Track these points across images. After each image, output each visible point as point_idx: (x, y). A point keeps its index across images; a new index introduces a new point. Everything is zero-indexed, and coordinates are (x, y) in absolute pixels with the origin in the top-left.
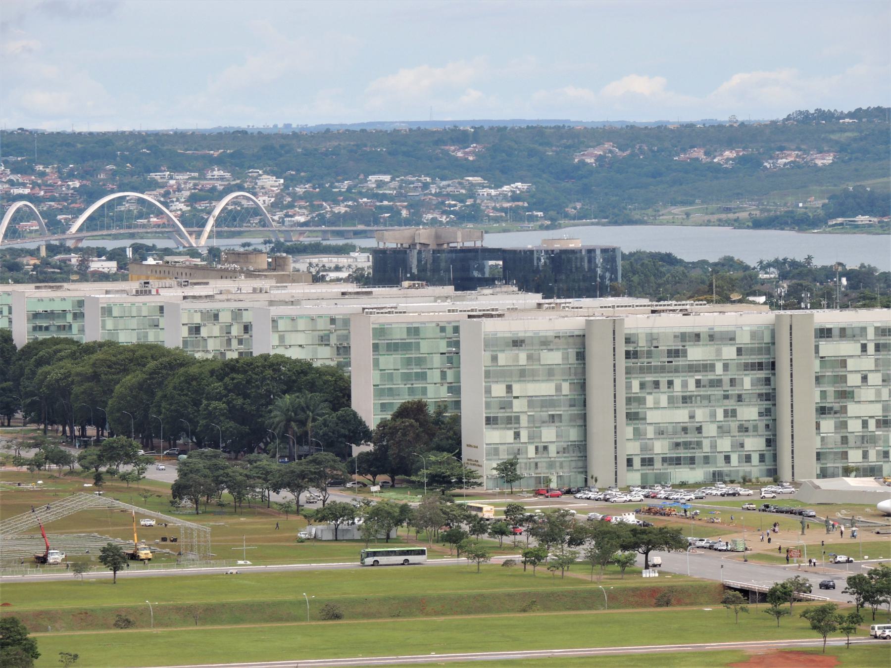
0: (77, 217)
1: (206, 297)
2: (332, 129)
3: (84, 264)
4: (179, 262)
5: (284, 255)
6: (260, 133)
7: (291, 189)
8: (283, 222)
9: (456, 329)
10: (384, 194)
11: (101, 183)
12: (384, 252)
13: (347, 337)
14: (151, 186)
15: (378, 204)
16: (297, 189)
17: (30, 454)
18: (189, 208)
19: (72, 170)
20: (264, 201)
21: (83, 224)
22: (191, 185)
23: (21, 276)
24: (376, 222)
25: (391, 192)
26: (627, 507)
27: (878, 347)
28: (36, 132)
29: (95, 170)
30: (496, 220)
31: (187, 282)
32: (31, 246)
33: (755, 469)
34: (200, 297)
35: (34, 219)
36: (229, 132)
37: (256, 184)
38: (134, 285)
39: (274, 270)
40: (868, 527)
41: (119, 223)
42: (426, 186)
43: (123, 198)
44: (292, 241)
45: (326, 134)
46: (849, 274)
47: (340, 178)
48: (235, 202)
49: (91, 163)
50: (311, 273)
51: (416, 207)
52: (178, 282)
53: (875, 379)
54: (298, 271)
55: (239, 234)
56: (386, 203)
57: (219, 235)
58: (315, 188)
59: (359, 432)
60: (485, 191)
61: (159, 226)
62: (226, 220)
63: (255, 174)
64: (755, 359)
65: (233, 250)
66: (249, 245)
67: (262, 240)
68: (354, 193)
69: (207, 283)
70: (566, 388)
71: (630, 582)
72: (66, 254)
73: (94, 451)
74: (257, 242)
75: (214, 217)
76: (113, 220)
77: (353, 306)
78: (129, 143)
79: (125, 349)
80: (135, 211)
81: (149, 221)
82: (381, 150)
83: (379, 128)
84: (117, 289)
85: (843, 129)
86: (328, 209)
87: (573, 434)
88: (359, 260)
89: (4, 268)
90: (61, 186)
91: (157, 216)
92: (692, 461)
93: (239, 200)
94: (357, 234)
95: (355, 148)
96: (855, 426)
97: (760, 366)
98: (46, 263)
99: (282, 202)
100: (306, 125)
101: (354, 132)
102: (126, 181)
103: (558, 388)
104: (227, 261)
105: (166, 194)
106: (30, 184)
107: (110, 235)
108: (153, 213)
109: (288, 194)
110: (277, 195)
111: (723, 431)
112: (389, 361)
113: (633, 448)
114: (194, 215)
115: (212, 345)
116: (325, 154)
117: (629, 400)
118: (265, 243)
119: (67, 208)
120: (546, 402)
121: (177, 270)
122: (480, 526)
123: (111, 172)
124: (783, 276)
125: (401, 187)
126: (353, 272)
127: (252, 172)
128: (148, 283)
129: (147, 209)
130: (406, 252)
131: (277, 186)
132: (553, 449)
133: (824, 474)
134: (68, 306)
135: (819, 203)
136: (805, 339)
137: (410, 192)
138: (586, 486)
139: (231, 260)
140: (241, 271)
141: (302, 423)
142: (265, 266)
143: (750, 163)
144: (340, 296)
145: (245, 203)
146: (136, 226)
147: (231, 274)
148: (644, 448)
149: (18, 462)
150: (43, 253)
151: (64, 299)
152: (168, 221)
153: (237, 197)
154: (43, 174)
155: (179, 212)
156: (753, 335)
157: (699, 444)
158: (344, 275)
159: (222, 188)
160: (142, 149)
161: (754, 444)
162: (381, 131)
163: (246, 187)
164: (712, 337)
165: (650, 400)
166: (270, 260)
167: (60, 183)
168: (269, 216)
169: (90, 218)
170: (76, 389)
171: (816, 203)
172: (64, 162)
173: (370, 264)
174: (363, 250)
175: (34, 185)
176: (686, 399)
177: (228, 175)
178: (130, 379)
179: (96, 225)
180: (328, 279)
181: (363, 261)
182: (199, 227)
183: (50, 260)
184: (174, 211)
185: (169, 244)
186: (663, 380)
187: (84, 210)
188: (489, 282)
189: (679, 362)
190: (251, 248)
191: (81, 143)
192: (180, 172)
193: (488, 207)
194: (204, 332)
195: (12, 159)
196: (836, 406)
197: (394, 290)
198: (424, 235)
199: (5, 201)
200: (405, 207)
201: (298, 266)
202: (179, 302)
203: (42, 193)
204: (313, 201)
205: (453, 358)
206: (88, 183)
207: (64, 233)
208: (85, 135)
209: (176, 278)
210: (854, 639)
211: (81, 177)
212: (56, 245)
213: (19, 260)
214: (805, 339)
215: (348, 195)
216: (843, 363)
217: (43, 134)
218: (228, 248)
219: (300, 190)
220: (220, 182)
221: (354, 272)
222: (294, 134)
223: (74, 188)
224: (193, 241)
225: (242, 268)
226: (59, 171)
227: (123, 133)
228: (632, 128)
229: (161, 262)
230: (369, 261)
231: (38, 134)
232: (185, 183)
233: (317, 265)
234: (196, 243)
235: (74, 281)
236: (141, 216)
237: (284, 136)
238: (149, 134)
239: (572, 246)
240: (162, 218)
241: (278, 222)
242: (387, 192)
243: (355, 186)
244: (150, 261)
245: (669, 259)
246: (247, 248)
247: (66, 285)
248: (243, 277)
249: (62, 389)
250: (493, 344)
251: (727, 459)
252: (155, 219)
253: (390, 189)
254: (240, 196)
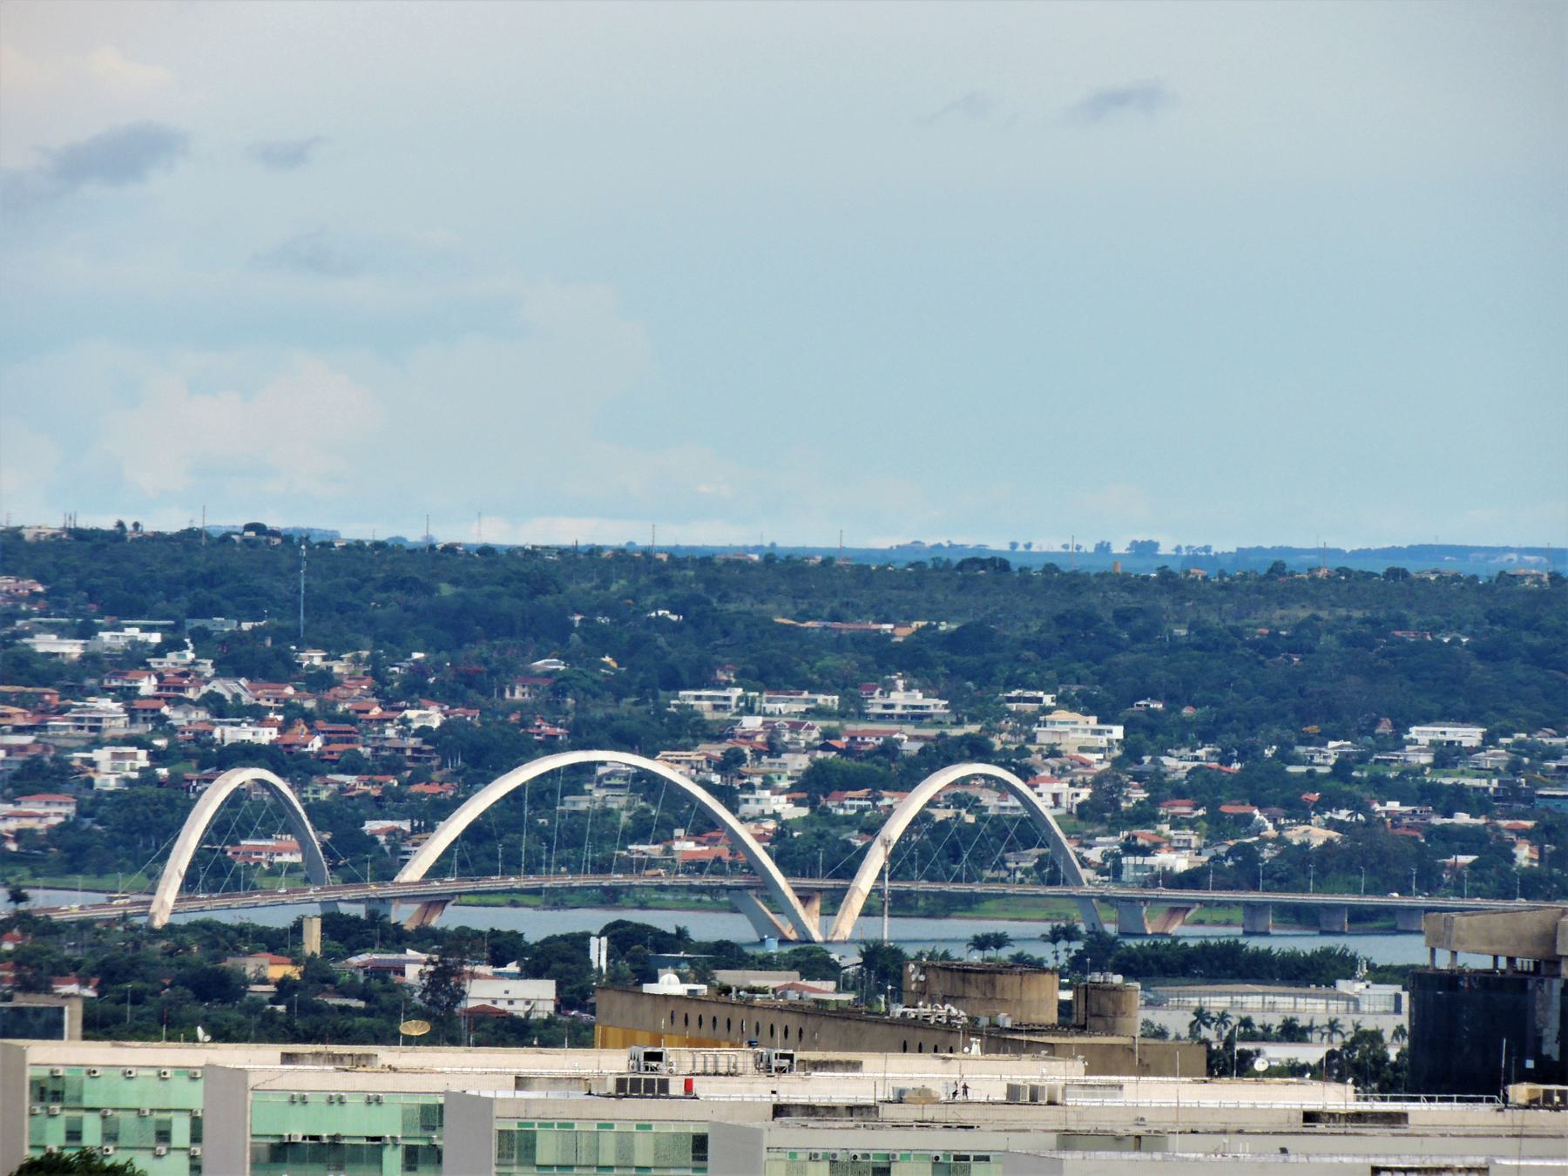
0: (431, 828)
1: (851, 1109)
2: (1291, 563)
3: (444, 982)
4: (763, 991)
5: (1118, 979)
6: (1050, 569)
7: (1147, 759)
8: (1117, 871)
10: (1459, 790)
11: (513, 718)
12: (1451, 980)
15: (1437, 821)
16: (1169, 762)
18: (804, 812)
19: (419, 670)
20: (1056, 797)
21: (447, 853)
22: (815, 734)
24: (1429, 881)
25: (1483, 783)
28: (306, 539)
29: (493, 673)
31: (791, 1057)
32: (277, 918)
34: (831, 1110)
35: (288, 830)
36: (948, 562)
37: (1032, 739)
38: (613, 1062)
39: (1082, 1029)
41: (566, 853)
43: (589, 767)
44: (1145, 935)
47: (1313, 729)
48: (958, 798)
49: (481, 649)
50: (1207, 1043)
52: (759, 1059)
54: (1161, 1034)
55: (968, 904)
56: (1462, 818)
57: (902, 905)
58: (1225, 760)
61: (699, 867)
62: (925, 855)
63: (1030, 707)
65: (946, 955)
66: (999, 941)
67: (1046, 928)
68: (1359, 781)
69: (855, 1066)
72: (389, 949)
75: (886, 843)
76: (549, 841)
78: (614, 588)
80: (624, 818)
81: (668, 851)
82: (1455, 641)
83: (1450, 566)
84: (557, 1072)
86: (1270, 831)
88: (1364, 1007)
89: (180, 989)
90: (381, 721)
91: (696, 834)
93: (973, 792)
94: (1362, 919)
95: (1366, 630)
98: (318, 975)
99: (1115, 804)
100: (1207, 549)
101: (1369, 576)
104: (923, 992)
105: (732, 762)
106: (278, 711)
107: (536, 892)
108: (683, 825)
109: (1138, 777)
110: (1098, 780)
114: (820, 836)
116: (1266, 648)
118: (1054, 937)
119: (398, 797)
121: (757, 1016)
123: (545, 684)
125: (1514, 768)
126: (1345, 1046)
127: (1019, 699)
128: (657, 1057)
130: (1524, 983)
131: (1101, 750)
134: (387, 1124)
137: (1545, 785)
139: (937, 989)
140: (972, 1029)
142: (1052, 1016)
144: (1298, 1124)
145: (991, 801)
146: (628, 866)
147: (938, 1037)
150: (313, 941)
151: (378, 1101)
152: (733, 853)
153: (964, 781)
154: (321, 681)
155: (771, 825)
158: (1312, 1053)
159: (915, 747)
160: (656, 608)
162: (1456, 578)
163: (998, 746)
166: (1067, 995)
167: (376, 711)
168: (1070, 847)
169: (474, 832)
172: (394, 641)
173: (1404, 1020)
174: (1380, 974)
175: (292, 714)
177: (937, 706)
179: (492, 856)
180: (1260, 1065)
182: (836, 876)
183: (335, 966)
184: (753, 819)
187: (455, 804)
190: (1005, 954)
191: (455, 582)
192: (776, 688)
195: (222, 625)
197: (1480, 1114)
199: (194, 764)
200: (1524, 834)
201: (1159, 1017)
202: (757, 1125)
203: (316, 743)
204: (1221, 803)
206: (472, 716)
207: (386, 873)
208: (467, 551)
209: (751, 1044)
211: (447, 695)
212: (357, 919)
213: (230, 963)
217: (327, 545)
218: (928, 948)
219: (1177, 764)
220: (910, 729)
221: (1350, 1047)
222: (1166, 576)
223: (423, 732)
224: (812, 921)
225: (973, 1020)
226: (377, 673)
227: (594, 551)
229: (702, 988)
230: (1398, 1010)
231: (310, 547)
232: (795, 727)
233: (1223, 1018)
234: (824, 929)
235: (410, 1041)
236: (642, 830)
237: (1128, 583)
238: (679, 560)
240: (713, 841)
241: (1101, 871)
242: (1468, 782)
243: (1362, 759)
244: (669, 984)
246: (991, 953)
247: (385, 1055)
248: (976, 1048)
252: (690, 846)
253: (1480, 772)
254: (974, 777)
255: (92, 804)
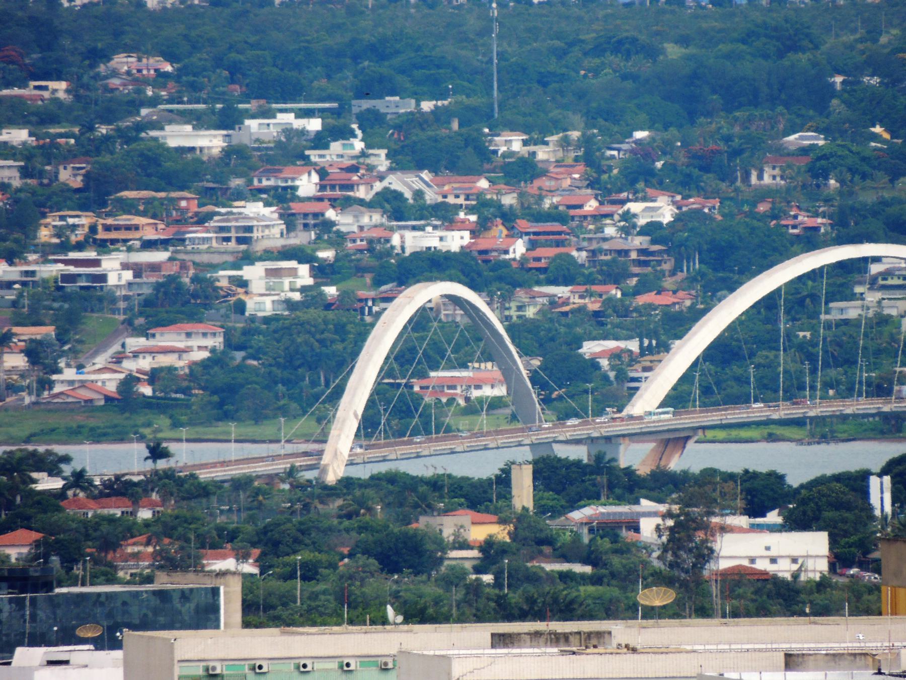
11: (762, 208)
19: (644, 151)
21: (686, 379)
23: (431, 590)
29: (737, 153)
35: (488, 357)
41: (833, 373)
43: (858, 266)
49: (721, 123)
72: (620, 500)
76: (812, 358)
78: (884, 40)
84: (837, 646)
89: (362, 559)
90: (598, 217)
102: (868, 197)
106: (470, 210)
107: (798, 423)
123: (803, 162)
167: (591, 206)
179: (742, 380)
183: (553, 524)
187: (695, 315)
191: (684, 41)
199: (368, 279)
203: (519, 248)
206: (710, 207)
212: (578, 464)
213: (423, 523)
223: (652, 229)
235: (651, 613)
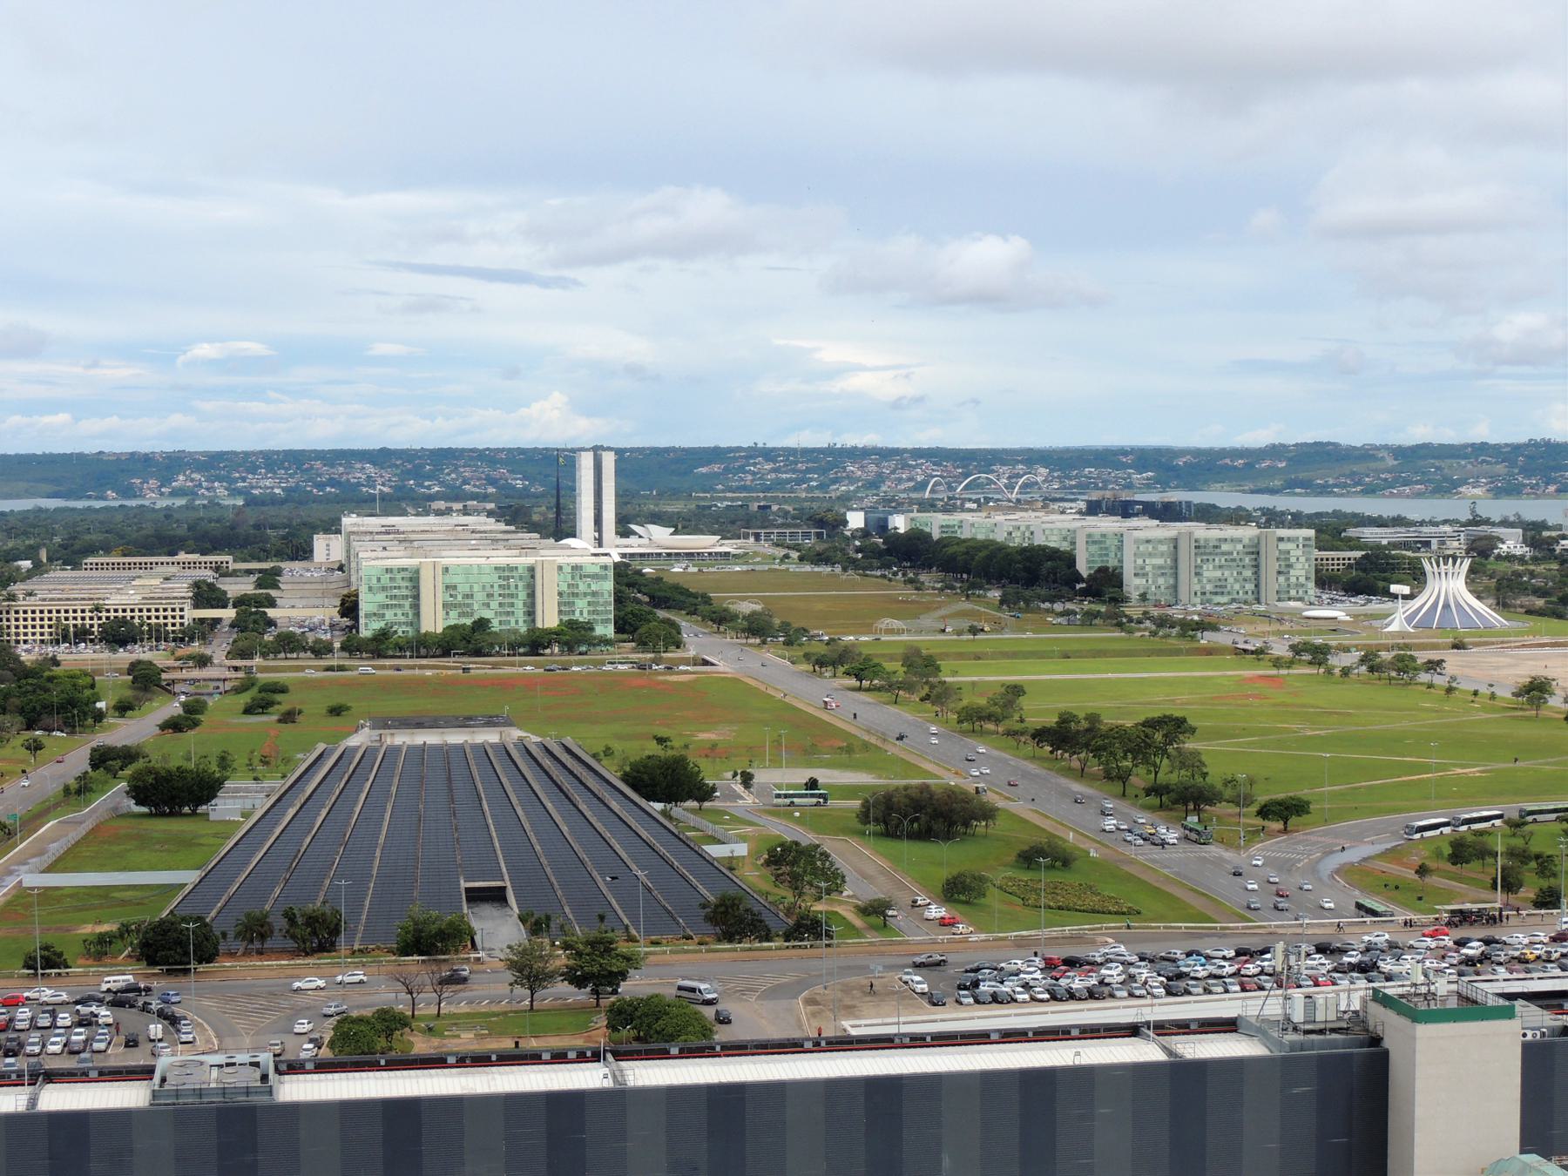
3: (963, 505)
9: (1122, 535)
13: (1075, 538)
14: (992, 472)
17: (939, 585)
24: (1088, 488)
26: (1194, 613)
27: (1304, 546)
30: (1140, 488)
33: (1250, 597)
38: (984, 514)
40: (1298, 624)
42: (1110, 473)
45: (1067, 450)
46: (1292, 514)
48: (1028, 479)
51: (1105, 482)
53: (1302, 559)
57: (1021, 493)
59: (1079, 579)
60: (1135, 476)
64: (1251, 550)
70: (1169, 561)
71: (1195, 645)
73: (966, 585)
74: (1036, 496)
77: (1078, 524)
79: (980, 541)
85: (1290, 451)
87: (1171, 581)
92: (1223, 593)
94: (1080, 493)
96: (1293, 580)
97: (1253, 553)
98: (947, 504)
103: (1166, 562)
111: (1236, 580)
112: (1093, 548)
113: (1197, 588)
115: (1017, 540)
117: (1196, 567)
120: (1160, 567)
122: (1130, 620)
124: (1264, 514)
129: (991, 482)
132: (1162, 587)
133: (1279, 600)
135: (1279, 483)
136: (1272, 542)
138: (1176, 604)
141: (1055, 574)
143: (1250, 466)
148: (1202, 587)
149: (934, 589)
156: (1250, 540)
157: (1226, 587)
158: (1074, 511)
161: (1250, 587)
164: (1232, 541)
165: (1205, 567)
170: (959, 558)
171: (1277, 483)
175: (942, 471)
176: (1220, 567)
178: (982, 554)
181: (1083, 505)
185: (1000, 497)
186: (1211, 558)
188: (1136, 515)
189: (1218, 551)
193: (1136, 483)
194: (1013, 535)
196: (1285, 571)
197: (1095, 518)
198: (1108, 494)
205: (1120, 548)
210: (1291, 671)
214: (1272, 542)
215: (1076, 477)
216: (1289, 553)
219: (1056, 474)
228: (1199, 449)
239: (1172, 500)
244: (991, 504)
245: (1214, 506)
249: (953, 558)
250: (1137, 541)
251: (1238, 593)
255: (917, 483)
